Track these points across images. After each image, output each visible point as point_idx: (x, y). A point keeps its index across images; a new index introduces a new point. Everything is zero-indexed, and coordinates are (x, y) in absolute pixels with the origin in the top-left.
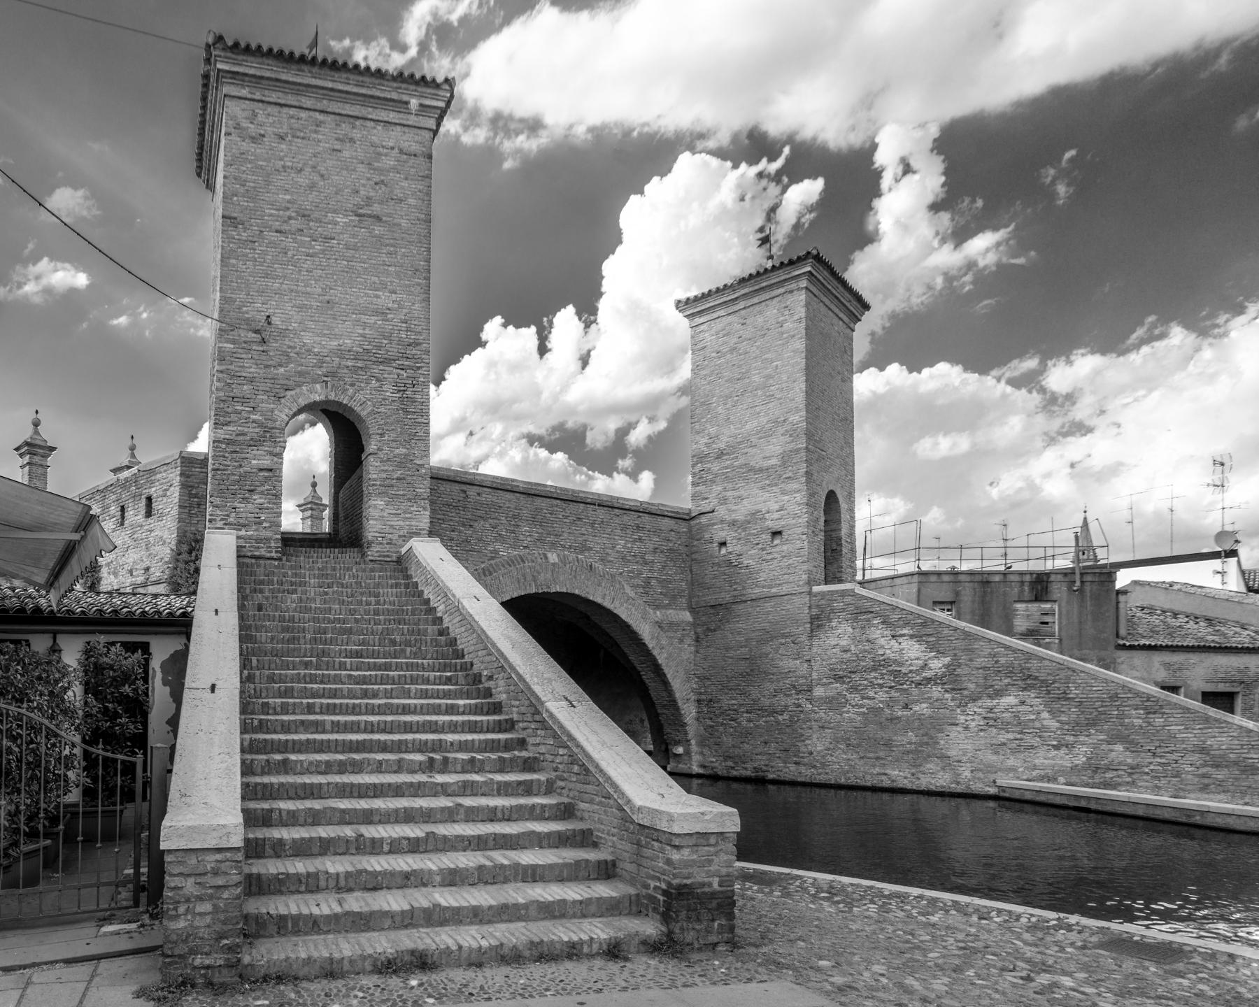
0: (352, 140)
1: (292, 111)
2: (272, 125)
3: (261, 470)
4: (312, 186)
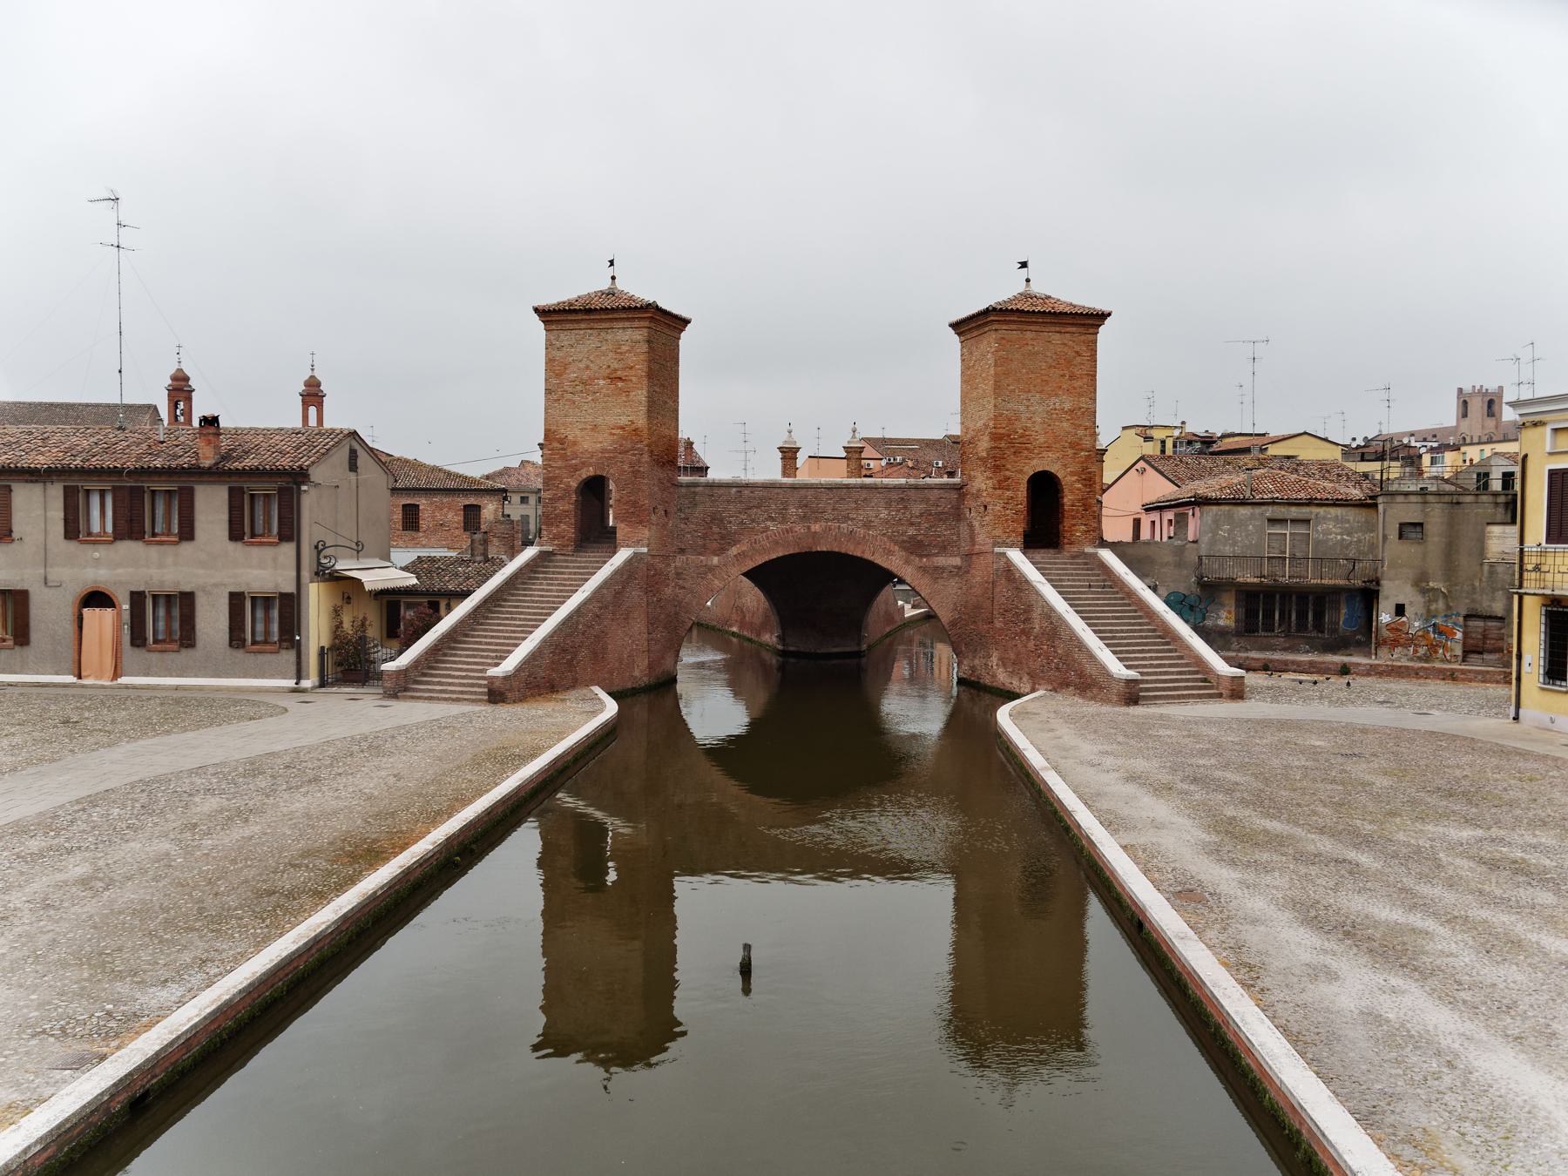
0: (607, 340)
1: (576, 332)
2: (567, 340)
3: (565, 511)
4: (587, 367)
